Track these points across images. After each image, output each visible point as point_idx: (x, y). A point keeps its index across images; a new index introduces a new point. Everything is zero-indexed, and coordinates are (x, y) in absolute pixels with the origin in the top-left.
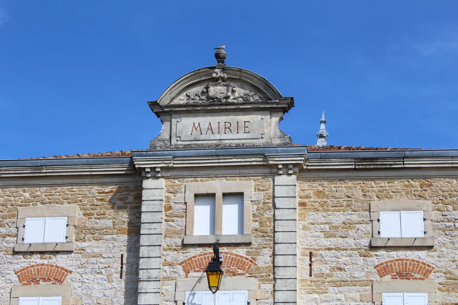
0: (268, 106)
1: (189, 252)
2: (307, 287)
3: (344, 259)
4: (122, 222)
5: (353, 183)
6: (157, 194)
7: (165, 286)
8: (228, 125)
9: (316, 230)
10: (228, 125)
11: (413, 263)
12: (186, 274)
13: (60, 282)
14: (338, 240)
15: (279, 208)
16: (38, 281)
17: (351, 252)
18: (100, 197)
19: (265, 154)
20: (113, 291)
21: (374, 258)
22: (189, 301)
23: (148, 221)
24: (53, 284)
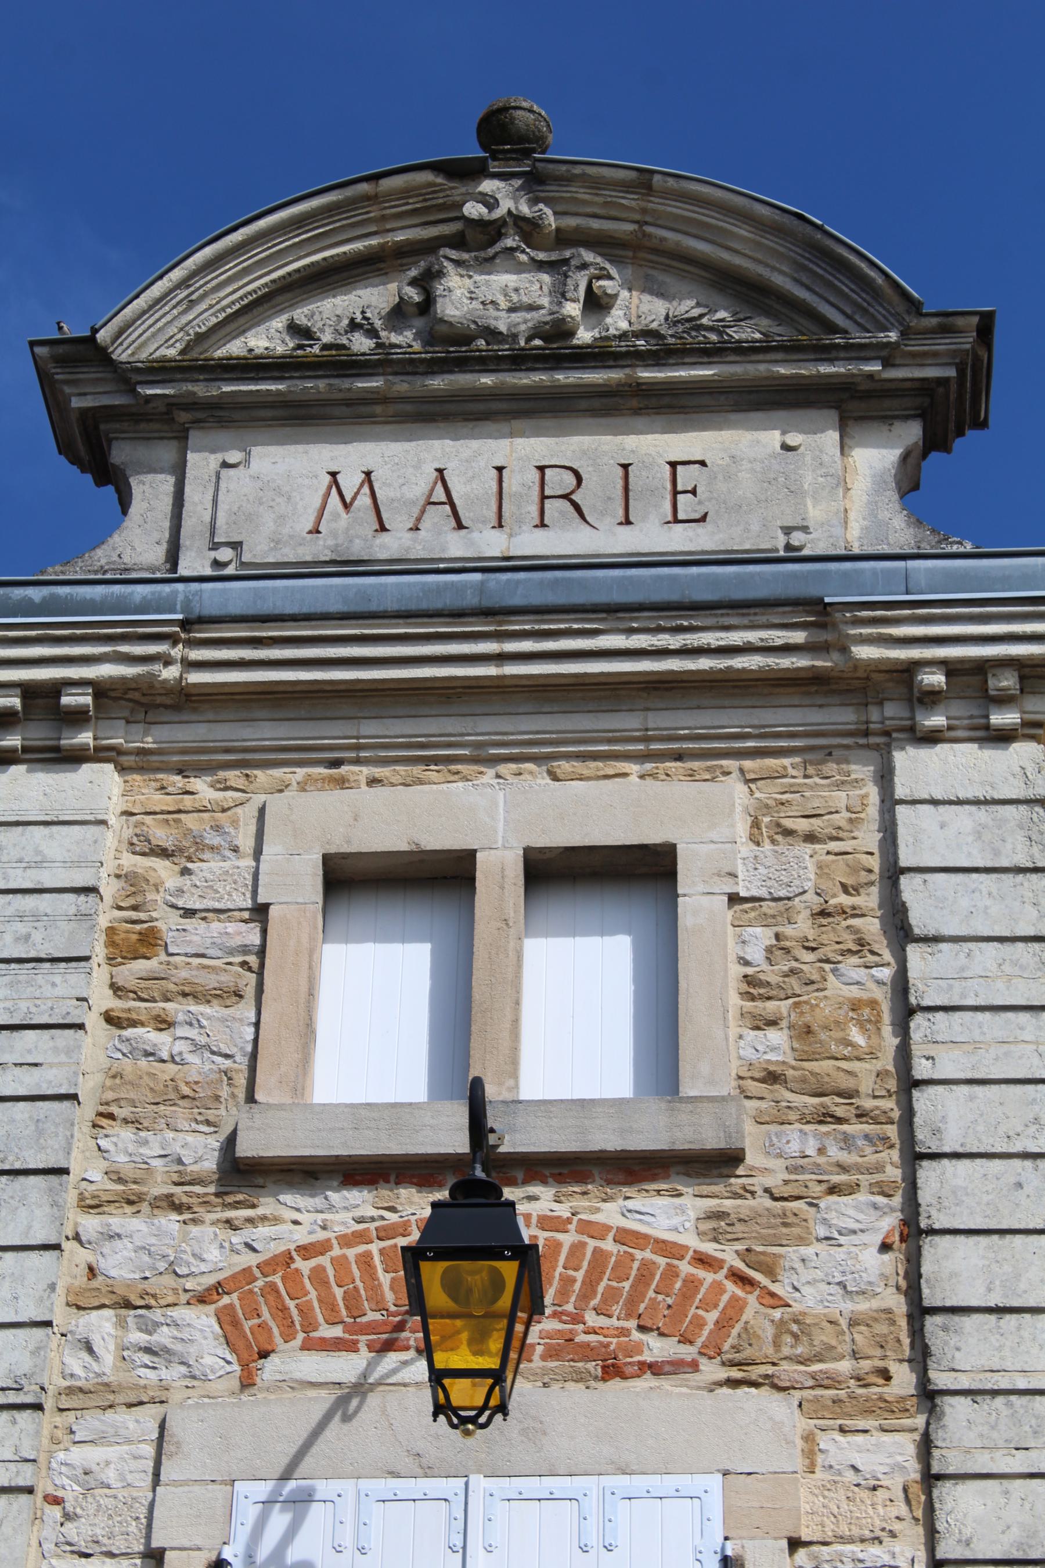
0: (825, 369)
1: (276, 1220)
7: (75, 1449)
10: (559, 481)
12: (245, 1366)
15: (932, 932)
19: (827, 600)
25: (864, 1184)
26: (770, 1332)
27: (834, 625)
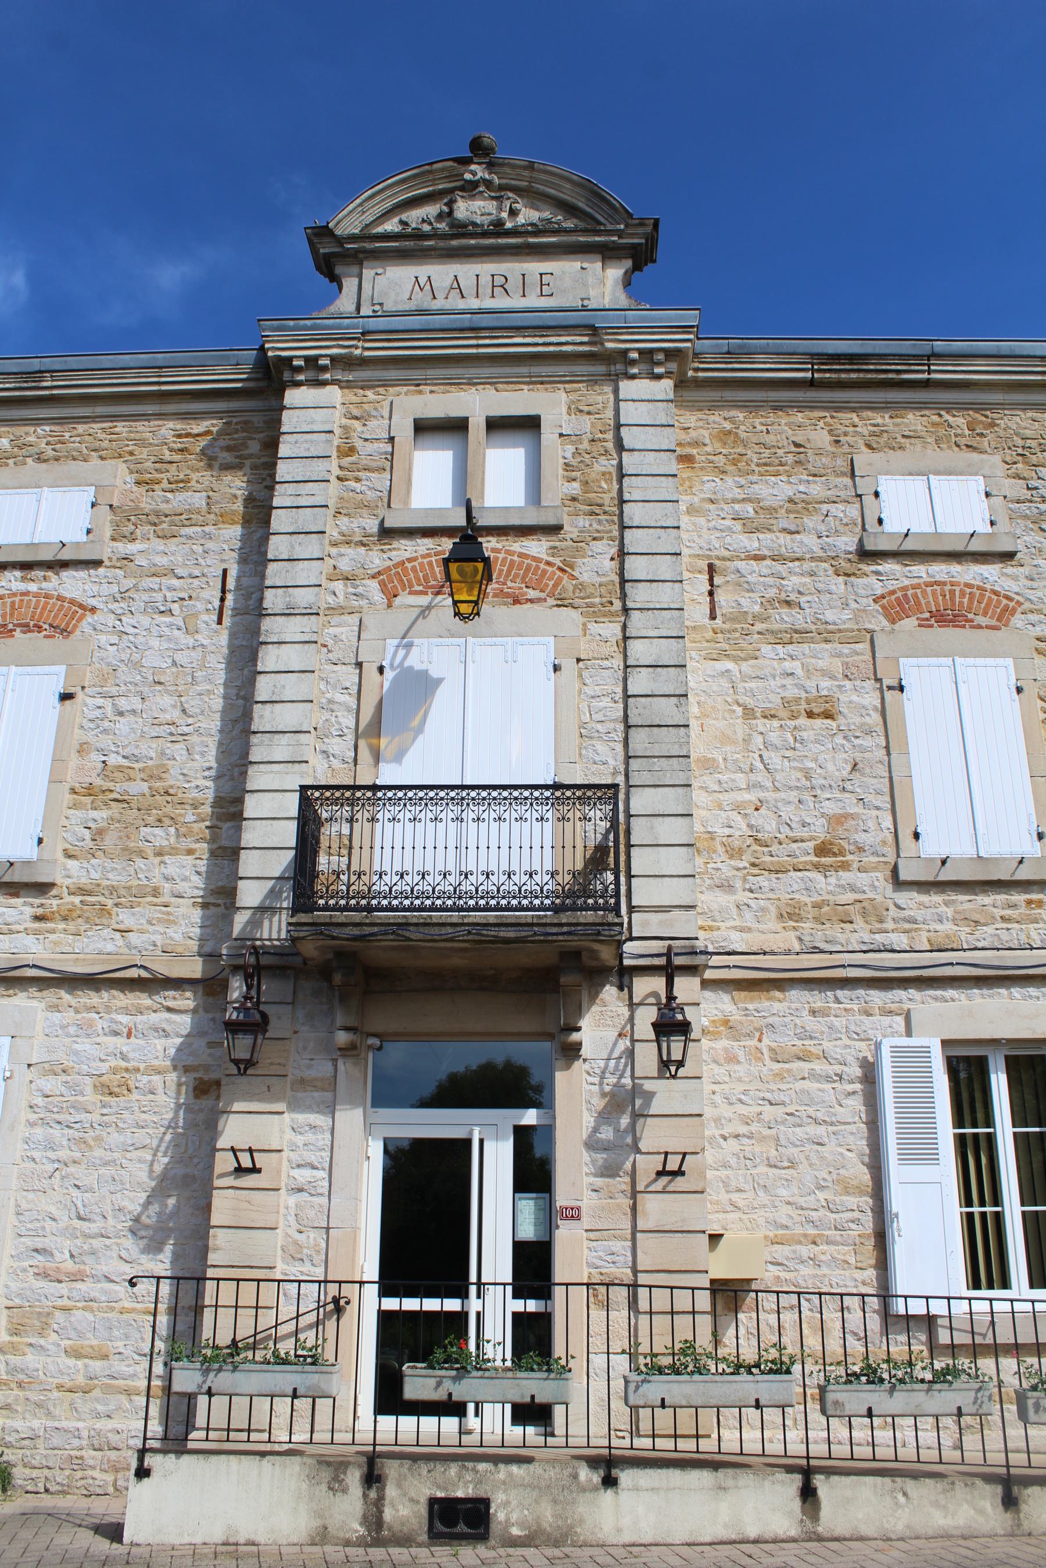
0: (597, 239)
1: (399, 549)
2: (705, 644)
3: (795, 580)
4: (229, 496)
6: (319, 419)
11: (968, 591)
12: (389, 600)
13: (65, 632)
16: (11, 631)
17: (813, 564)
20: (196, 655)
22: (396, 663)
24: (46, 637)
26: (571, 588)
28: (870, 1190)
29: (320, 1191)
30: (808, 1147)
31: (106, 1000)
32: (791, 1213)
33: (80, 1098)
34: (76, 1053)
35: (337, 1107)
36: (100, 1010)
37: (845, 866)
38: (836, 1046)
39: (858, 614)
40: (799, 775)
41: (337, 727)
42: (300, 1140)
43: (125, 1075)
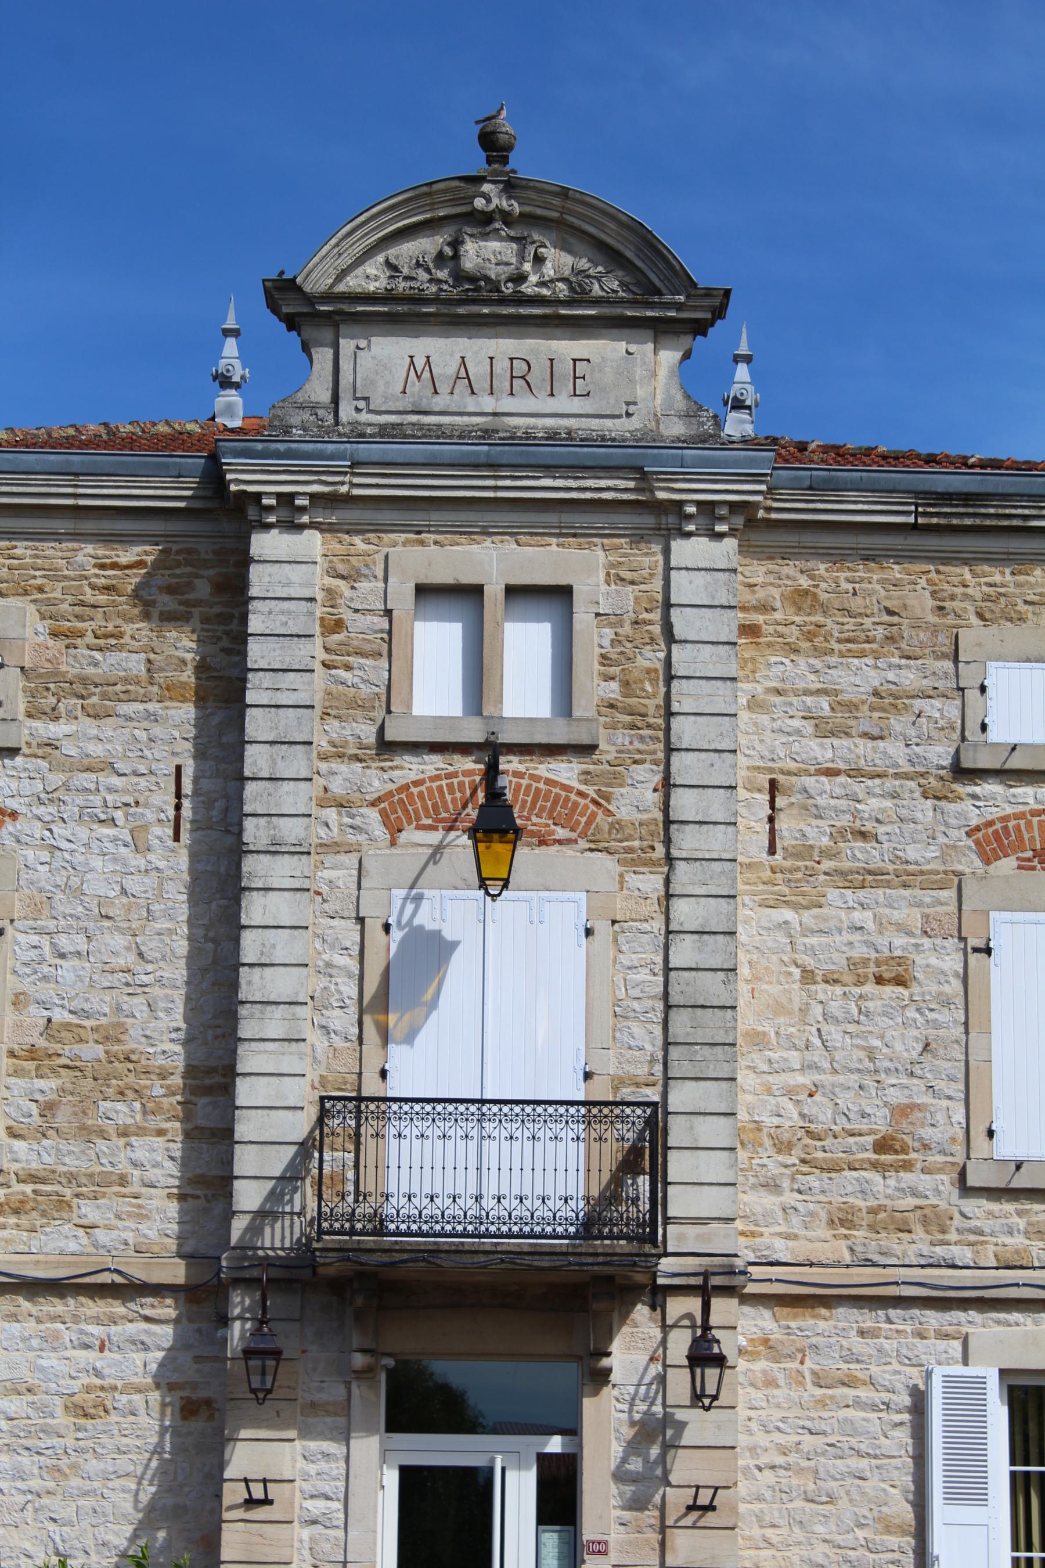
1: (402, 768)
2: (761, 887)
3: (874, 803)
5: (904, 568)
8: (520, 367)
9: (791, 713)
10: (520, 367)
12: (392, 836)
14: (856, 746)
15: (683, 638)
17: (897, 783)
18: (103, 580)
19: (646, 469)
21: (967, 805)
23: (269, 664)
25: (648, 760)
26: (606, 828)
27: (648, 479)
28: (912, 1530)
29: (335, 1523)
30: (849, 1481)
31: (72, 1308)
32: (827, 1551)
33: (49, 1421)
34: (42, 1369)
35: (353, 1435)
36: (67, 1320)
37: (907, 1166)
38: (884, 1372)
39: (948, 851)
40: (862, 1054)
41: (337, 996)
42: (312, 1469)
43: (100, 1394)
